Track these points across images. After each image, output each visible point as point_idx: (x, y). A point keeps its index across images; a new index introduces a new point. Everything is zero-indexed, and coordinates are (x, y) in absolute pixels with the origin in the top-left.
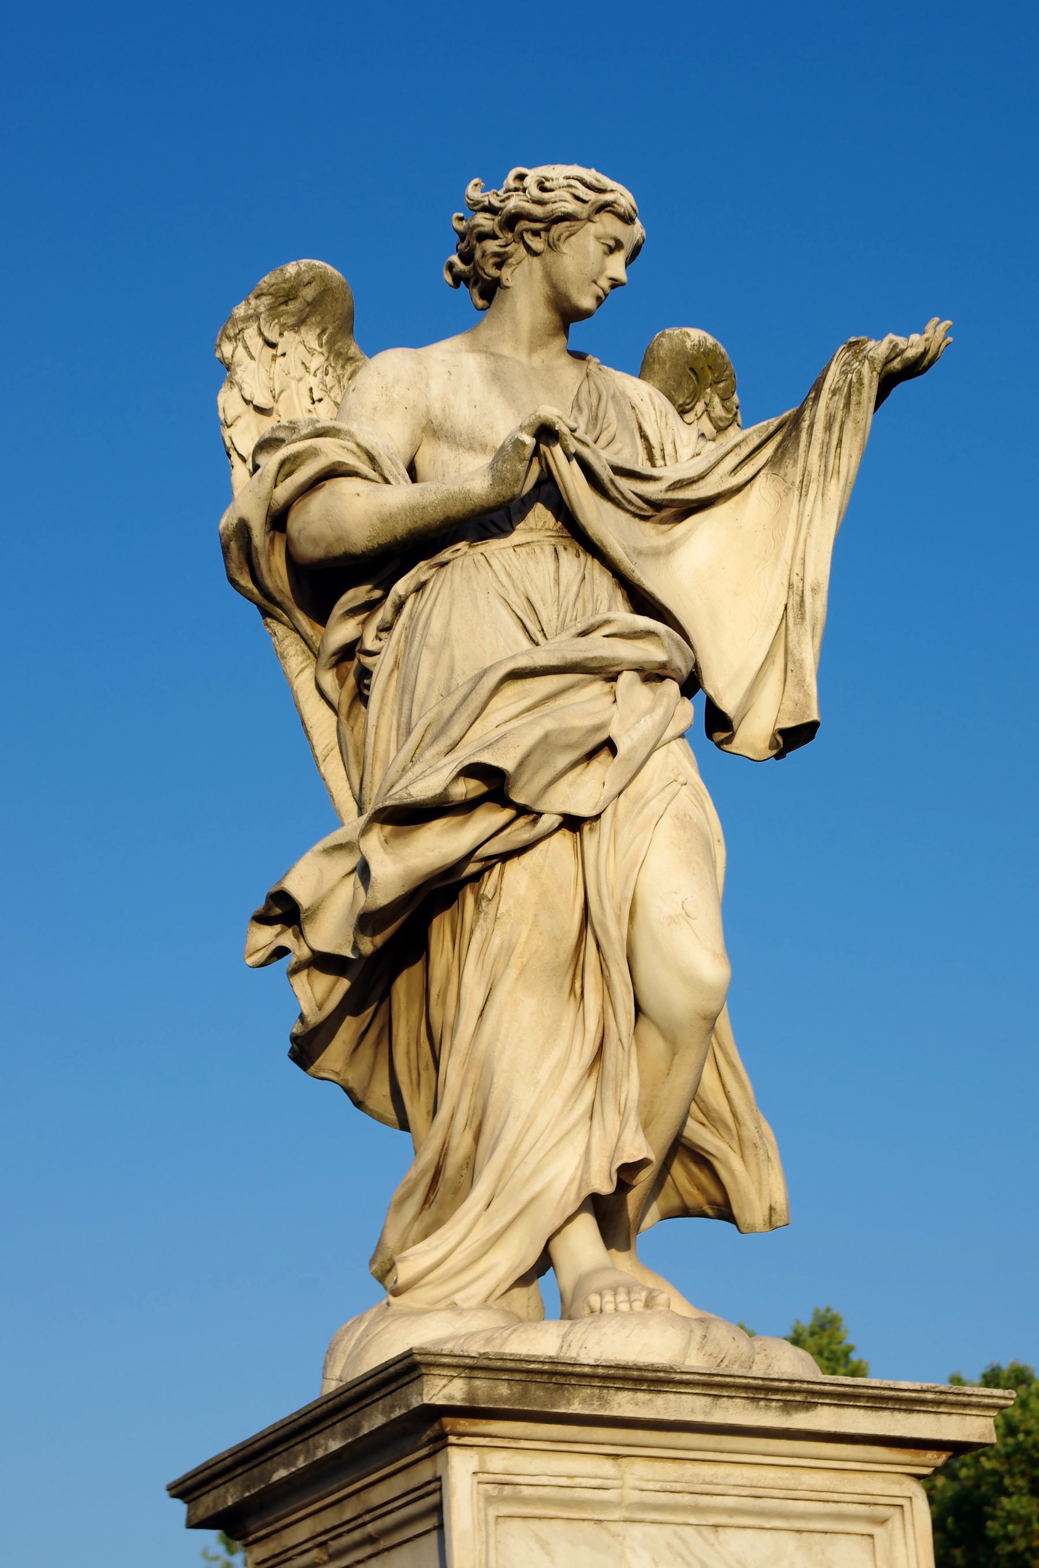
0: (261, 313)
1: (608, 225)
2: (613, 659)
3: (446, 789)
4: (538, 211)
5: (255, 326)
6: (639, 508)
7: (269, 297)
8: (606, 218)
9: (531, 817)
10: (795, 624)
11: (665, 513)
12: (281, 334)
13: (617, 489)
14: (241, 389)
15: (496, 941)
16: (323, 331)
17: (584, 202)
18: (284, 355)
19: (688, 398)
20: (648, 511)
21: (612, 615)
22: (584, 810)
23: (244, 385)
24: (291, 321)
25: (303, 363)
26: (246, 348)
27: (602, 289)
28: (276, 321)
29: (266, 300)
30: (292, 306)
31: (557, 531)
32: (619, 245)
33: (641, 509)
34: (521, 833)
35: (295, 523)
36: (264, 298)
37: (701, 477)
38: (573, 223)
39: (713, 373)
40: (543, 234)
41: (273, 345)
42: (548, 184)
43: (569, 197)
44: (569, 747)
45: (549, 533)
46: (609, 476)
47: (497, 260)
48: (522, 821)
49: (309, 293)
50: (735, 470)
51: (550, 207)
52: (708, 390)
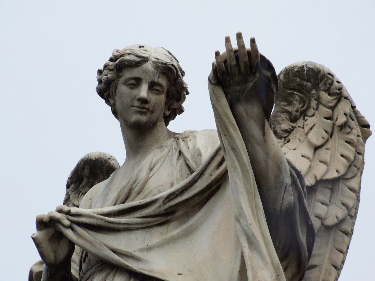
1: (128, 74)
5: (71, 203)
6: (149, 223)
11: (178, 214)
19: (300, 104)
27: (137, 107)
28: (81, 193)
33: (153, 222)
49: (86, 171)
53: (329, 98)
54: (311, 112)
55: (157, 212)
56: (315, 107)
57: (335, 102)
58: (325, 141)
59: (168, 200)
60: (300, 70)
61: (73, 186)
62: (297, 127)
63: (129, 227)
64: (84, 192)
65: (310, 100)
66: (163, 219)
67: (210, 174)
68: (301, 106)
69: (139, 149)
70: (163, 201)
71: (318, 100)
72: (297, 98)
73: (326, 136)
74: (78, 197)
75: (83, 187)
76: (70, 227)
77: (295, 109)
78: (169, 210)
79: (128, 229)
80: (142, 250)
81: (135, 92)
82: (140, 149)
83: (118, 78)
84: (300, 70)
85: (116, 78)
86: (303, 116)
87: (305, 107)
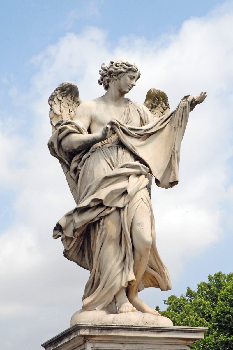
1: (132, 74)
3: (89, 204)
4: (116, 71)
6: (137, 136)
8: (130, 72)
9: (109, 208)
10: (173, 159)
13: (131, 133)
14: (53, 111)
15: (104, 233)
16: (72, 97)
17: (126, 69)
18: (63, 102)
23: (54, 110)
24: (65, 95)
25: (68, 104)
26: (54, 102)
29: (59, 91)
30: (64, 92)
31: (118, 143)
34: (108, 212)
35: (63, 143)
37: (152, 128)
39: (162, 98)
40: (117, 76)
41: (61, 101)
42: (118, 65)
43: (122, 68)
44: (117, 193)
45: (116, 144)
47: (108, 81)
48: (107, 209)
49: (68, 89)
50: (161, 125)
51: (118, 70)
54: (157, 108)
66: (140, 137)
72: (157, 101)
77: (155, 105)
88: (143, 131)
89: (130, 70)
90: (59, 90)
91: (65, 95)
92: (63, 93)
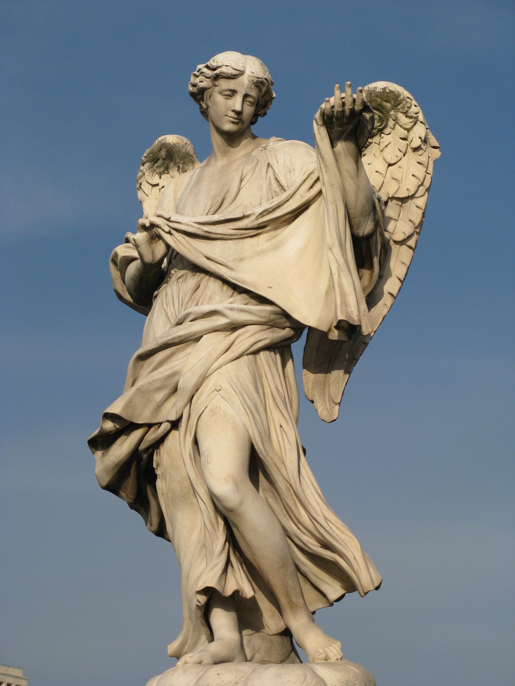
0: (145, 173)
1: (224, 85)
2: (188, 334)
6: (241, 234)
7: (148, 163)
9: (157, 426)
12: (160, 178)
18: (163, 187)
19: (378, 122)
20: (252, 233)
21: (189, 310)
22: (173, 417)
24: (162, 169)
28: (155, 172)
29: (147, 165)
30: (160, 162)
32: (234, 92)
33: (245, 234)
34: (153, 435)
36: (146, 164)
38: (208, 91)
39: (390, 103)
41: (157, 185)
44: (159, 389)
46: (203, 231)
48: (152, 430)
49: (163, 153)
50: (311, 187)
52: (392, 113)
53: (407, 120)
54: (387, 131)
55: (249, 226)
56: (392, 127)
57: (412, 124)
58: (398, 159)
59: (261, 216)
60: (382, 91)
61: (148, 165)
62: (373, 143)
63: (224, 237)
64: (159, 171)
65: (388, 120)
66: (255, 232)
67: (301, 196)
68: (379, 124)
69: (227, 153)
70: (258, 216)
71: (396, 120)
73: (400, 155)
74: (152, 175)
75: (157, 167)
76: (169, 233)
78: (261, 225)
79: (223, 238)
80: (234, 260)
81: (230, 102)
82: (228, 153)
83: (214, 86)
84: (382, 91)
85: (212, 87)
86: (380, 133)
87: (383, 126)
88: (253, 218)
89: (217, 77)
90: (147, 161)
91: (162, 169)
92: (157, 167)
